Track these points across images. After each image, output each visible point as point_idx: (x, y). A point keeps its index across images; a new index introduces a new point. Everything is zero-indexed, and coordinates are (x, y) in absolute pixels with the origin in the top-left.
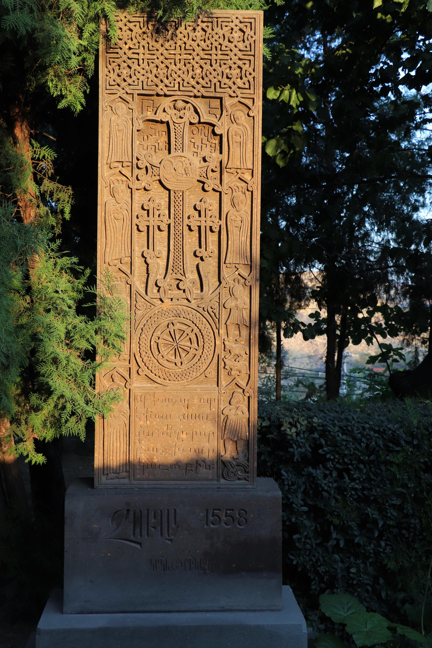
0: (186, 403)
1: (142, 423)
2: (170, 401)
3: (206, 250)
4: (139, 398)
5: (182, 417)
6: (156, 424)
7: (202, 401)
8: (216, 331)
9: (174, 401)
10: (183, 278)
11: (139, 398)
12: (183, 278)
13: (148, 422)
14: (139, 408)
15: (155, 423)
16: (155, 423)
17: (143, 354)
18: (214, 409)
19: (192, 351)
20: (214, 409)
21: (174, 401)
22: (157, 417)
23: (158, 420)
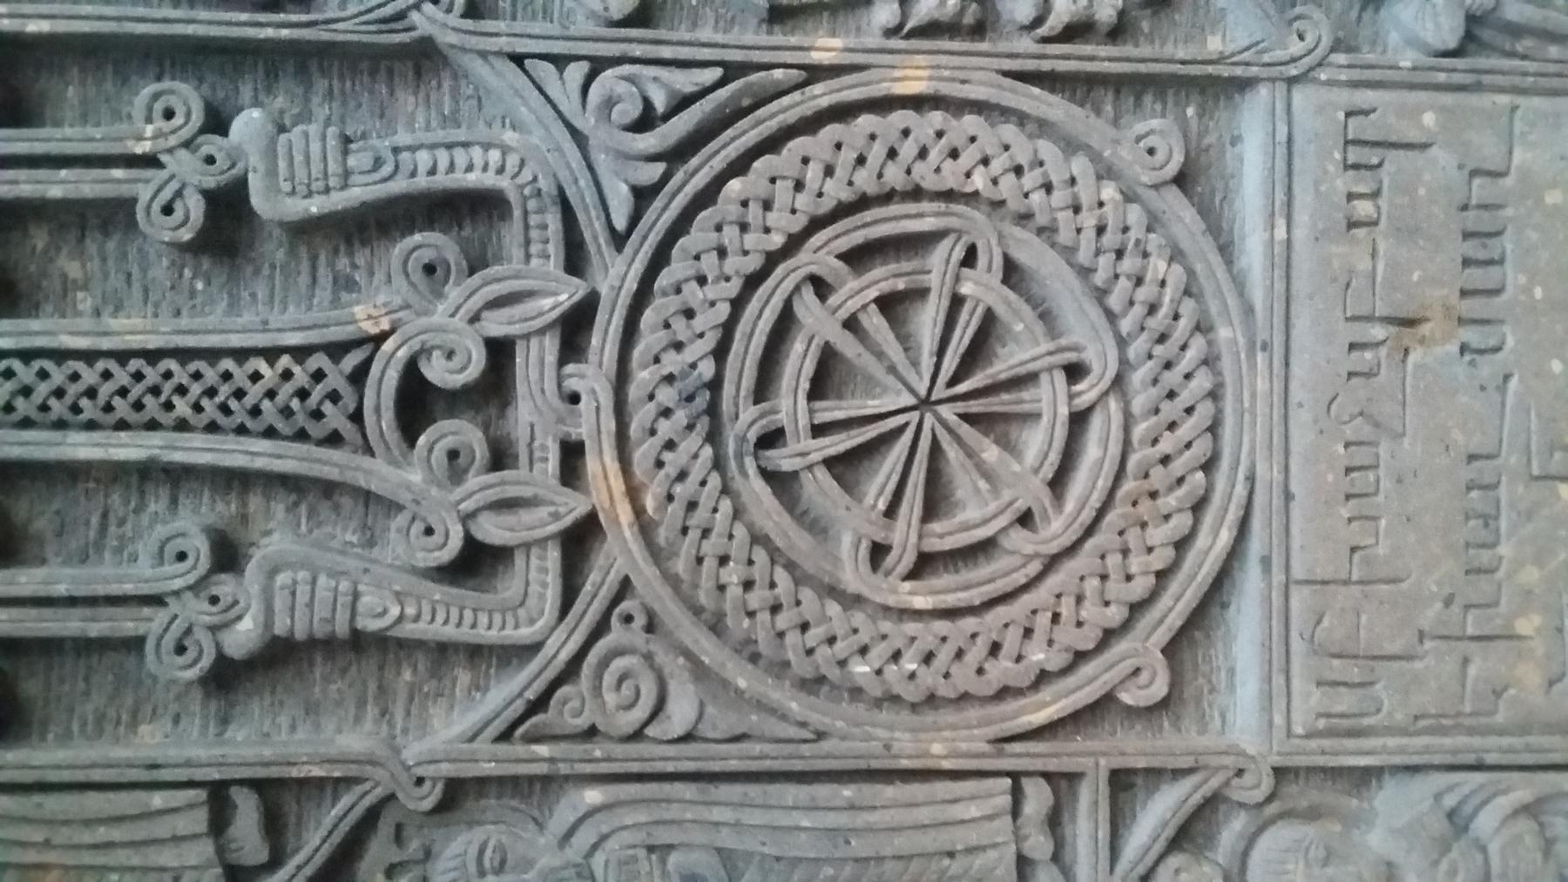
0: (1378, 332)
1: (1530, 676)
2: (1361, 456)
3: (151, 161)
4: (1345, 701)
5: (1488, 368)
6: (1539, 561)
7: (1364, 208)
8: (822, 95)
9: (1367, 432)
10: (394, 354)
11: (1345, 701)
12: (394, 354)
13: (1524, 626)
14: (1425, 700)
15: (1531, 575)
16: (1531, 575)
17: (1002, 670)
18: (1429, 119)
19: (983, 287)
20: (1429, 119)
21: (1367, 432)
22: (1485, 557)
23: (1504, 549)
